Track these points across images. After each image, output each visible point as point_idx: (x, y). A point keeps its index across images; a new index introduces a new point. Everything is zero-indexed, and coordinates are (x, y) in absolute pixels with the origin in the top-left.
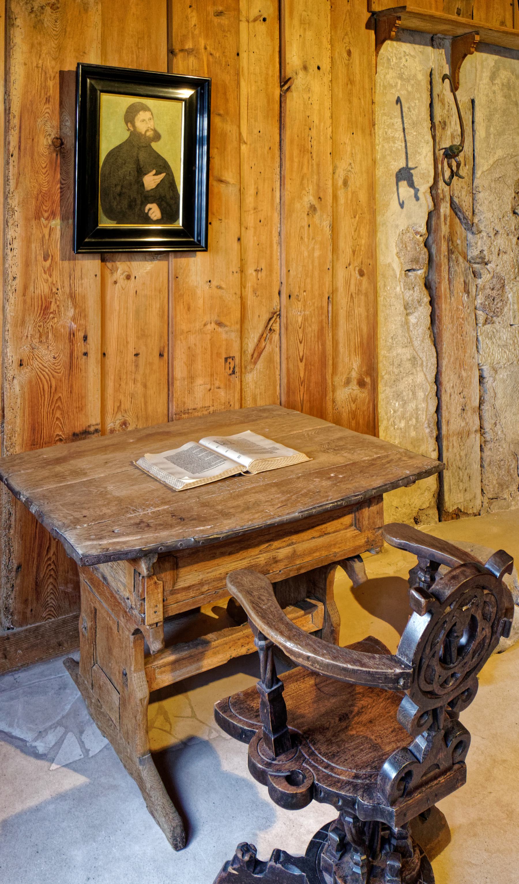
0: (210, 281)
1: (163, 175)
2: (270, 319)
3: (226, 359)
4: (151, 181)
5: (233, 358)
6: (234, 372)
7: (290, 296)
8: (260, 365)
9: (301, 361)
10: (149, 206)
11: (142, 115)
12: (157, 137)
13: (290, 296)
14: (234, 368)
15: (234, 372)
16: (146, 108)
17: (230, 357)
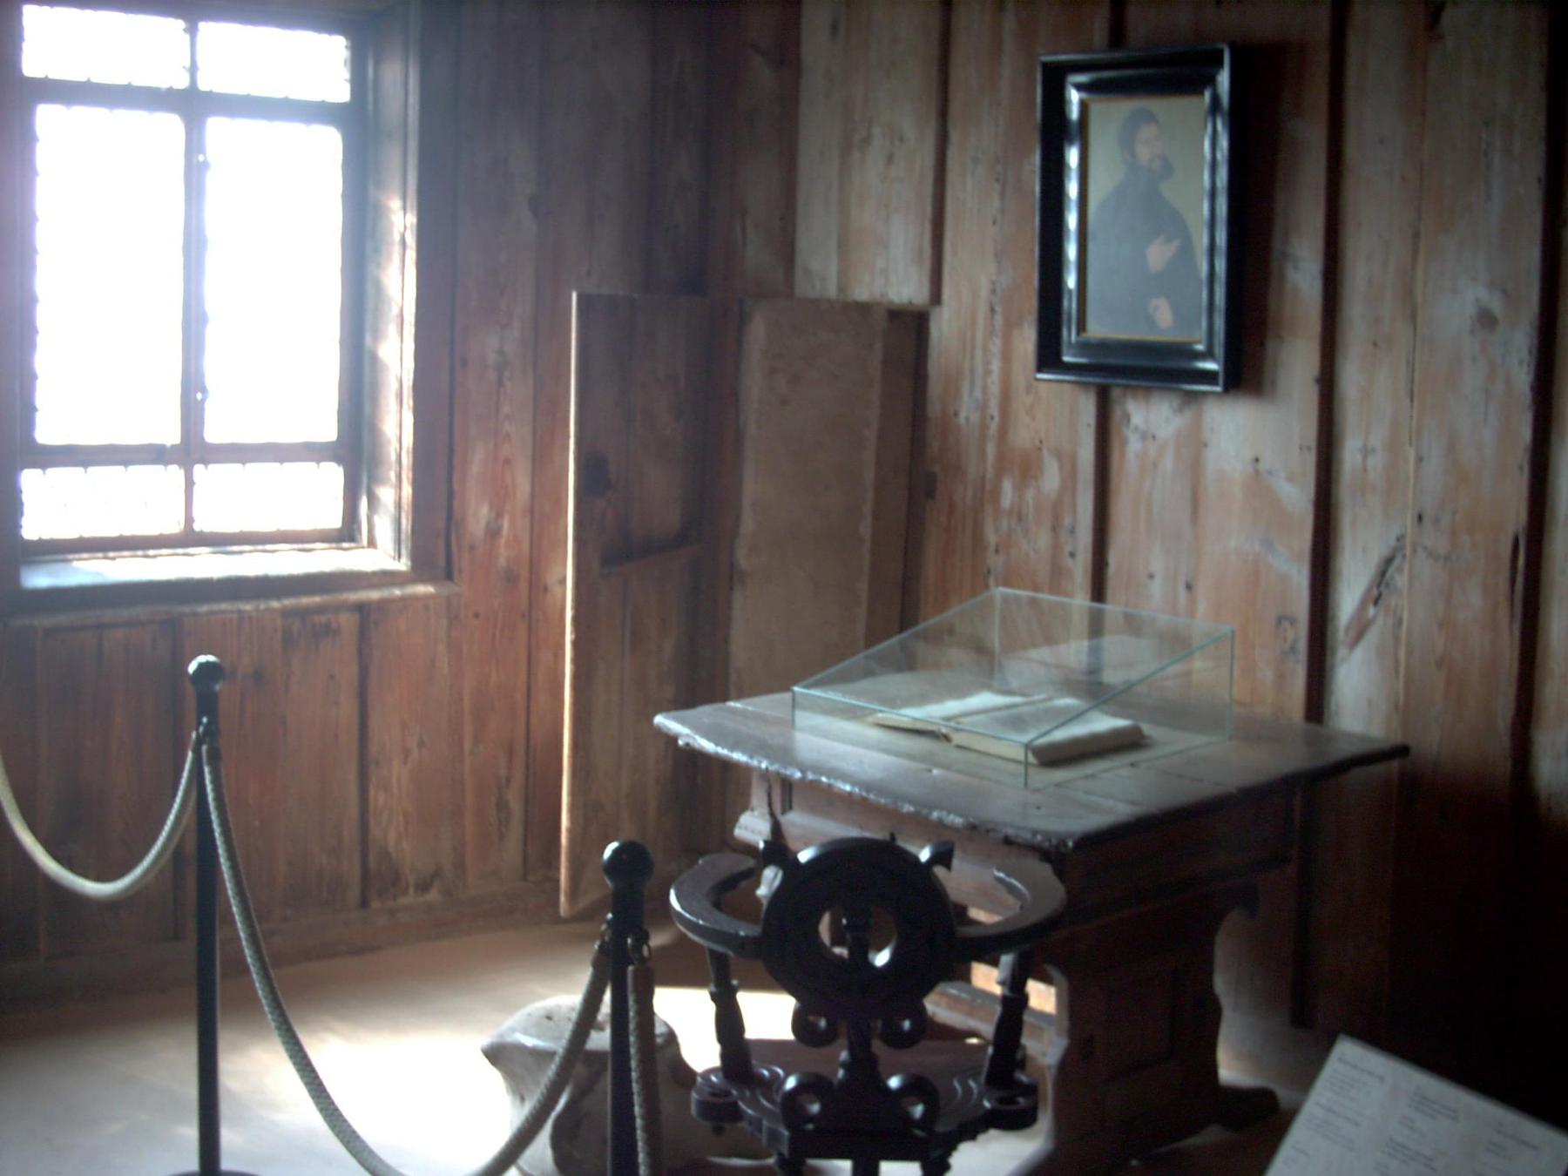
0: (1257, 460)
1: (1176, 243)
2: (1389, 561)
3: (1279, 620)
4: (1158, 254)
5: (1293, 622)
6: (1293, 649)
7: (1420, 518)
8: (1359, 654)
9: (1439, 665)
10: (1155, 302)
11: (1147, 131)
12: (1167, 169)
13: (1420, 518)
14: (1295, 641)
15: (1293, 649)
16: (1151, 118)
17: (1286, 618)
